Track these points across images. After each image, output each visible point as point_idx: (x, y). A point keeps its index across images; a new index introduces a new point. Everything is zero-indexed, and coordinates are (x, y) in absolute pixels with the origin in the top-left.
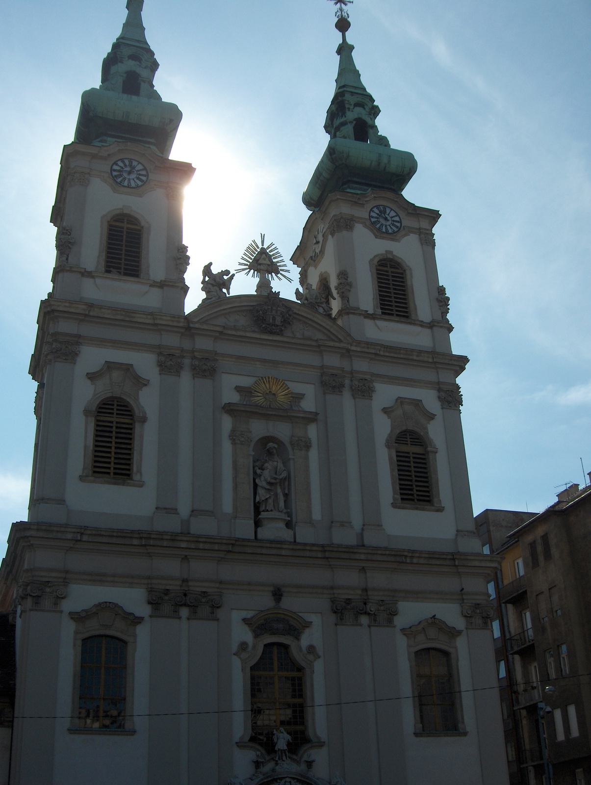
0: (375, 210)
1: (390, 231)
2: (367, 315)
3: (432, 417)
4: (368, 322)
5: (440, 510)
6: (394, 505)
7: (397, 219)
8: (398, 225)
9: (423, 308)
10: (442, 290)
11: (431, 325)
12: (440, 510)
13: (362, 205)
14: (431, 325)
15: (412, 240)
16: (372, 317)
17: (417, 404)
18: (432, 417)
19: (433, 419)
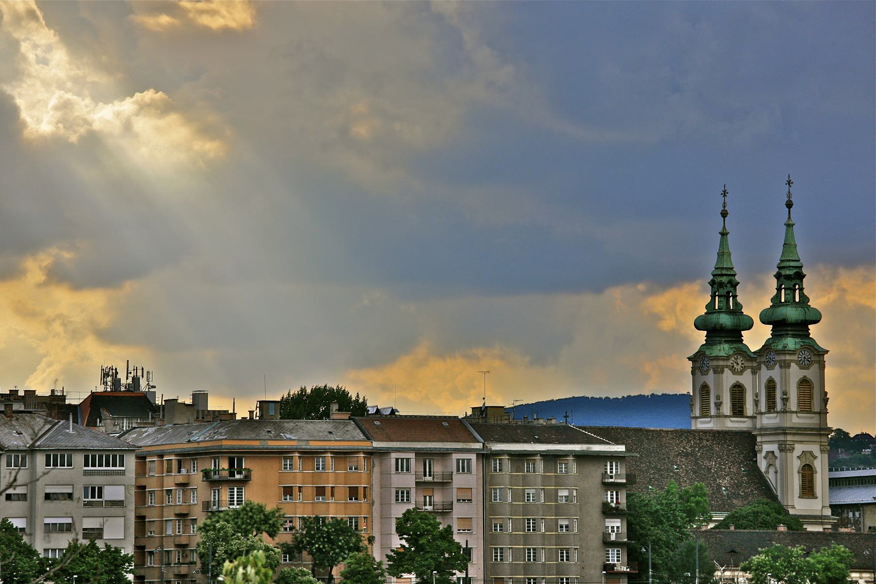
0: (801, 354)
1: (806, 364)
2: (793, 412)
3: (815, 458)
4: (794, 415)
5: (817, 498)
6: (799, 497)
7: (809, 357)
8: (809, 360)
9: (816, 406)
10: (826, 393)
11: (819, 413)
12: (817, 498)
13: (796, 354)
14: (819, 413)
15: (815, 367)
16: (796, 412)
17: (811, 453)
18: (815, 458)
19: (815, 458)
